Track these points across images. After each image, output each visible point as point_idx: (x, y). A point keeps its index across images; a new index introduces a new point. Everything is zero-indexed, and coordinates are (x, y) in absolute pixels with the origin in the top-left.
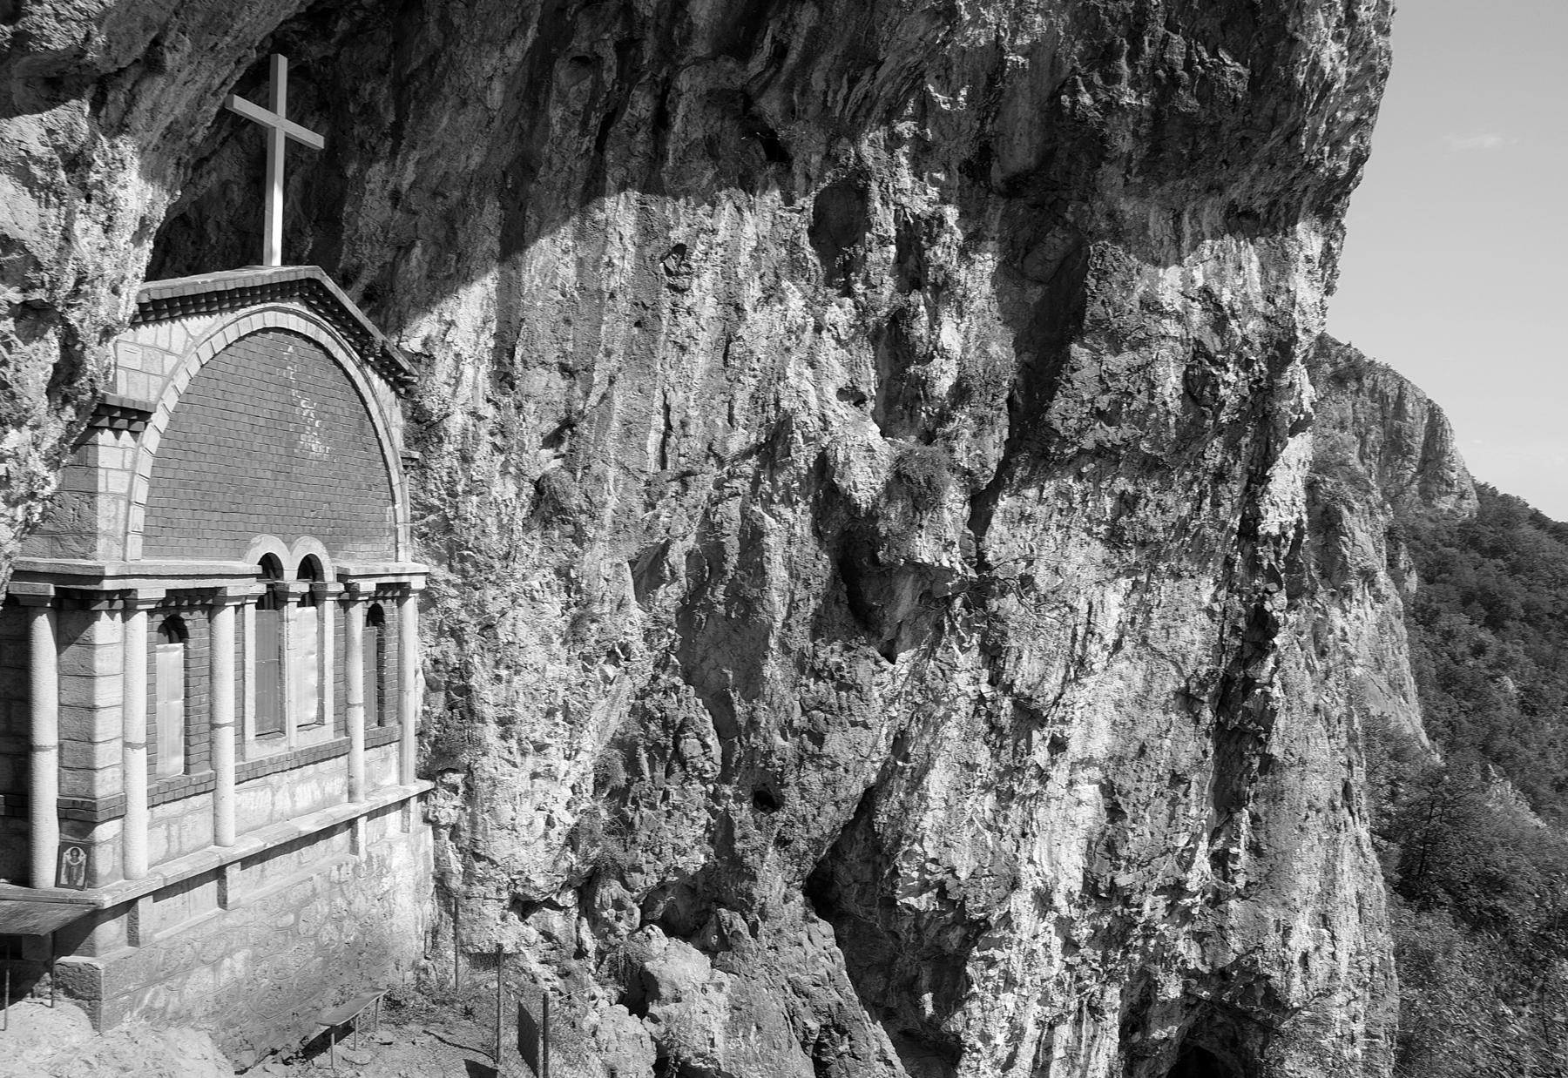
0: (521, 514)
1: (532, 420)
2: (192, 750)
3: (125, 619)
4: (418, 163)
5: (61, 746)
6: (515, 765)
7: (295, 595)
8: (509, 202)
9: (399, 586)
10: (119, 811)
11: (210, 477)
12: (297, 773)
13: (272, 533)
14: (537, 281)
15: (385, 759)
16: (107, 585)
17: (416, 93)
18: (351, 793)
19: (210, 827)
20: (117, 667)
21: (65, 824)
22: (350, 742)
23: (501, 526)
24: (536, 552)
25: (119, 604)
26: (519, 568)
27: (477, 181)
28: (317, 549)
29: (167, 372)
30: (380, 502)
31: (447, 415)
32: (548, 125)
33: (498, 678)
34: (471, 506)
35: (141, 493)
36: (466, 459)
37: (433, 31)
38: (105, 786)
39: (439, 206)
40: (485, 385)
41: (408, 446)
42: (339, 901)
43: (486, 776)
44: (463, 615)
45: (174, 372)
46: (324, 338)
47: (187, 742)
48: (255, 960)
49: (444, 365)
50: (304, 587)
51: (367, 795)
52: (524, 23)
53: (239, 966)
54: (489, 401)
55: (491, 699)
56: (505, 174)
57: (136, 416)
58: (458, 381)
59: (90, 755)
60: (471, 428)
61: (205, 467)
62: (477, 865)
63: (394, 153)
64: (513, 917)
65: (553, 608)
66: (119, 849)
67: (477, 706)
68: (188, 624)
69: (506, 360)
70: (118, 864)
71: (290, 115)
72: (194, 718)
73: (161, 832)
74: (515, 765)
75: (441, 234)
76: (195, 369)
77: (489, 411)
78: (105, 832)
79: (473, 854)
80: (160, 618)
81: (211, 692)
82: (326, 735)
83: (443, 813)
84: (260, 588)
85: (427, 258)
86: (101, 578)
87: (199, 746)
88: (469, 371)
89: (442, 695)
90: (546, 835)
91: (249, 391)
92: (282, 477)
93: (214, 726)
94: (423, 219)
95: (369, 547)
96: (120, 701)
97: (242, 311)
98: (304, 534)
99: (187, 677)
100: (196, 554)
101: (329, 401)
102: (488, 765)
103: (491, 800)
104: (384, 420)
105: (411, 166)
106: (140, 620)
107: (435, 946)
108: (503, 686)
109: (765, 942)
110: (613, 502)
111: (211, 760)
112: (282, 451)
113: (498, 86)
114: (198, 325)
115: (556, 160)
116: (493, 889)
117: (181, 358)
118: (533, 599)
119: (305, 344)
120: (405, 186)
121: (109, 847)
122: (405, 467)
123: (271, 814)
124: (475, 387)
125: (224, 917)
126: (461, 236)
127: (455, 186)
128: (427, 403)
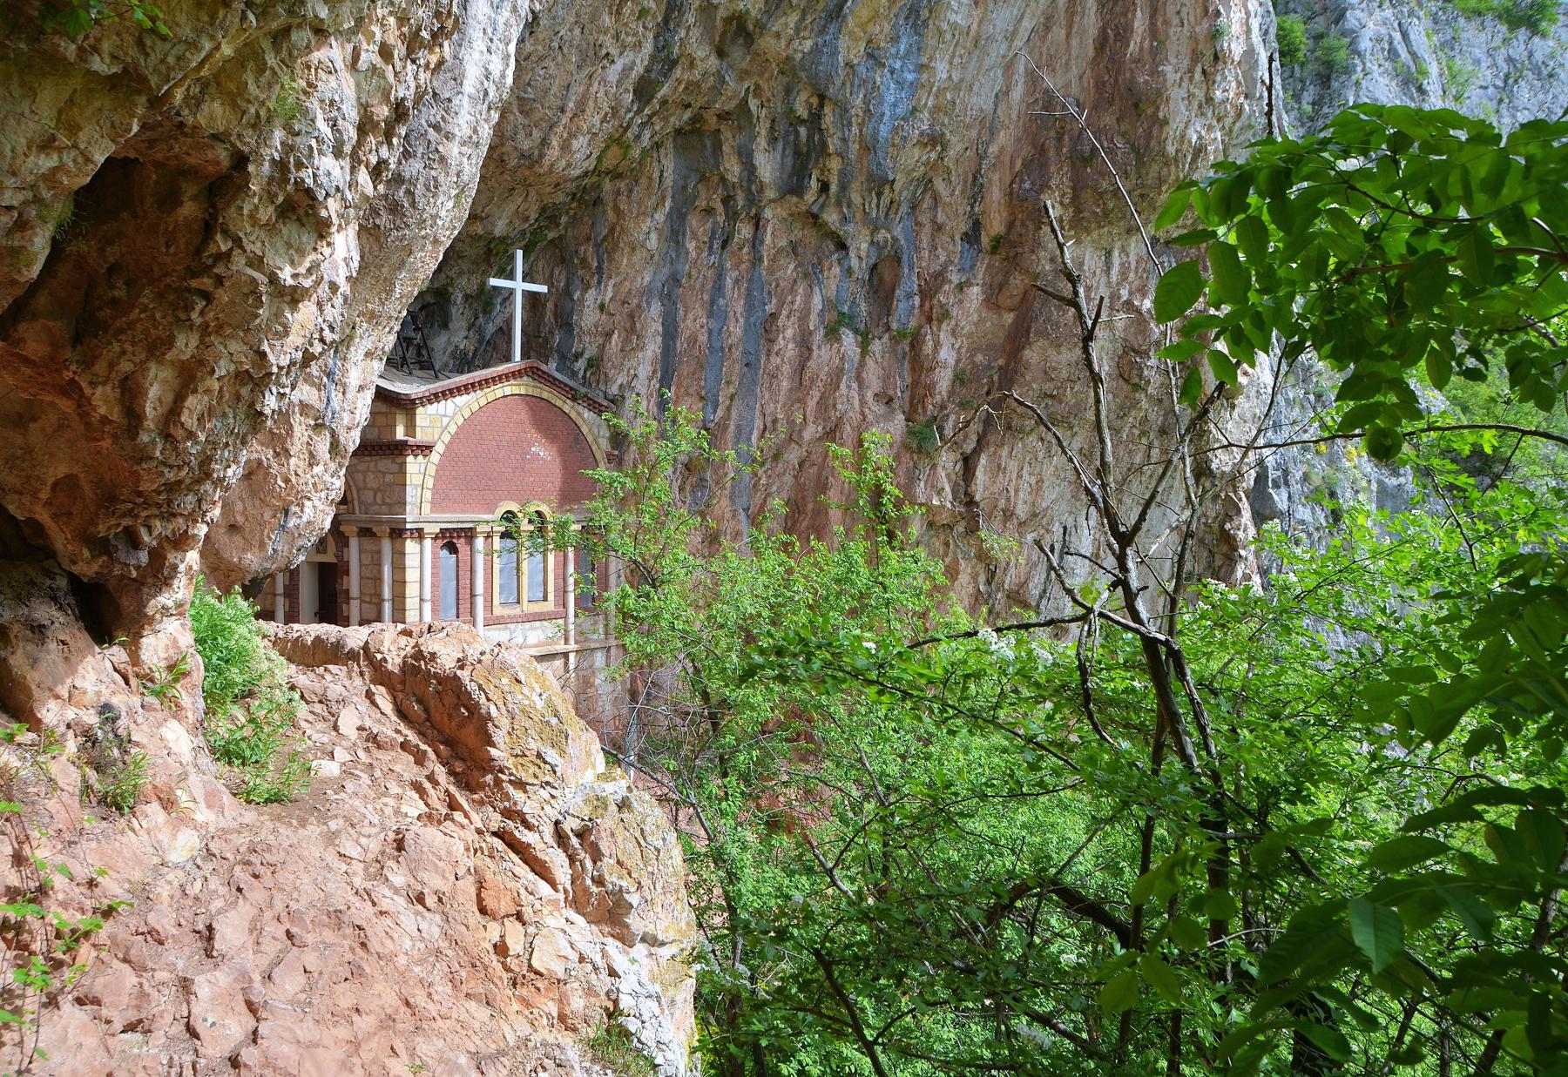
3: (421, 543)
12: (528, 625)
15: (595, 623)
16: (408, 526)
18: (566, 641)
27: (647, 292)
28: (544, 508)
35: (430, 483)
37: (611, 215)
39: (626, 309)
46: (545, 395)
52: (664, 198)
57: (426, 449)
59: (404, 604)
63: (599, 282)
71: (524, 280)
76: (460, 421)
80: (440, 543)
82: (549, 606)
87: (465, 606)
93: (473, 596)
94: (618, 317)
100: (463, 512)
105: (610, 288)
106: (428, 543)
111: (472, 613)
113: (654, 236)
114: (460, 400)
115: (694, 272)
117: (452, 418)
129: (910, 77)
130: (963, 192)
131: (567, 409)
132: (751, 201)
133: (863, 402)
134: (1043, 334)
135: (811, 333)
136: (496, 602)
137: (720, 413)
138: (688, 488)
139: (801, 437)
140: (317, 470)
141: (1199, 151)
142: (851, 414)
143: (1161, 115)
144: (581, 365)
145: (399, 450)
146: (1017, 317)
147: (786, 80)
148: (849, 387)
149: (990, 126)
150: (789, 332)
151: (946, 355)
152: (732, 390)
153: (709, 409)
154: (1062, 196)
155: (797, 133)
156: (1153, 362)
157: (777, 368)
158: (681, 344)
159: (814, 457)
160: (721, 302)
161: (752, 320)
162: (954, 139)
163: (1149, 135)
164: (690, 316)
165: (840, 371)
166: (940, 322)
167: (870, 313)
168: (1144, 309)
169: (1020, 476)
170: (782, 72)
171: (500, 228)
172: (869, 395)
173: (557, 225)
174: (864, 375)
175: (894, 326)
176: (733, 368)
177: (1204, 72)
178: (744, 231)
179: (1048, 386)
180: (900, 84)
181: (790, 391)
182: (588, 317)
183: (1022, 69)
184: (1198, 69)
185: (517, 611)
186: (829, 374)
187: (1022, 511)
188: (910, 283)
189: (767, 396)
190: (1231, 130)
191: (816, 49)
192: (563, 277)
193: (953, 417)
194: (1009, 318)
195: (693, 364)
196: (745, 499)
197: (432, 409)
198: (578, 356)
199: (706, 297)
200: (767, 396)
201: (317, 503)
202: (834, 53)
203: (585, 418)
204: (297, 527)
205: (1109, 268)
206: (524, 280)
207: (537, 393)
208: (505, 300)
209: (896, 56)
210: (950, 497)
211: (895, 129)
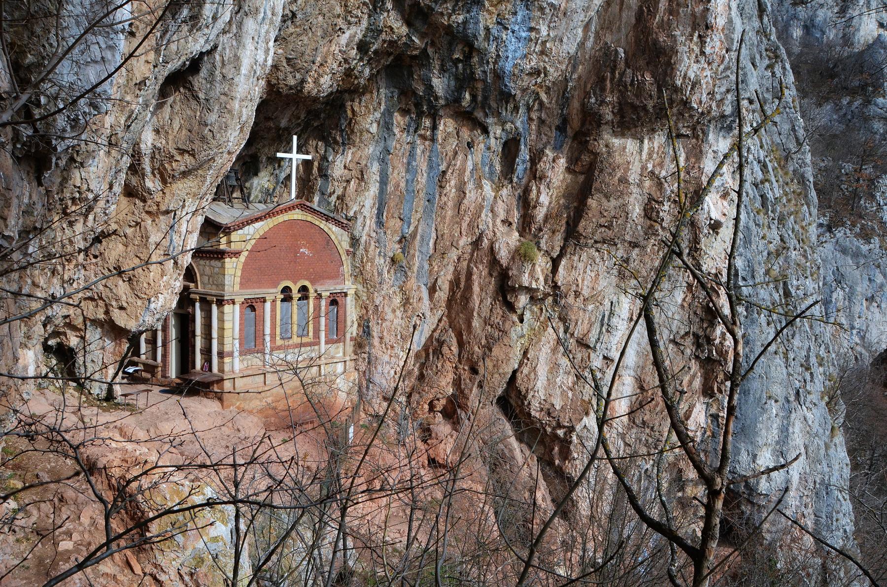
1: (389, 237)
4: (352, 153)
10: (231, 354)
15: (338, 347)
16: (226, 298)
20: (231, 318)
23: (378, 273)
26: (385, 287)
28: (307, 283)
34: (368, 267)
35: (239, 273)
36: (366, 251)
37: (349, 113)
38: (227, 348)
40: (374, 226)
46: (309, 219)
49: (360, 220)
57: (237, 254)
59: (223, 340)
62: (371, 385)
63: (344, 151)
65: (397, 300)
71: (297, 153)
77: (374, 235)
78: (227, 360)
79: (369, 381)
84: (282, 296)
87: (259, 341)
88: (368, 222)
93: (264, 335)
94: (354, 172)
100: (259, 288)
105: (350, 155)
106: (237, 307)
110: (417, 264)
114: (257, 225)
115: (398, 146)
128: (355, 233)
129: (524, 34)
130: (556, 102)
132: (431, 106)
133: (494, 225)
134: (599, 191)
135: (465, 183)
136: (278, 338)
138: (392, 271)
139: (458, 244)
141: (695, 84)
142: (487, 232)
143: (672, 61)
144: (333, 199)
145: (220, 255)
146: (586, 178)
147: (449, 38)
148: (487, 216)
149: (573, 61)
150: (453, 183)
151: (544, 199)
152: (419, 215)
154: (613, 108)
155: (457, 68)
156: (666, 208)
157: (445, 203)
158: (390, 188)
159: (466, 255)
160: (414, 163)
161: (431, 175)
162: (552, 70)
163: (665, 74)
164: (396, 172)
165: (481, 207)
166: (540, 179)
167: (502, 171)
168: (662, 176)
169: (585, 272)
170: (447, 34)
171: (284, 123)
172: (498, 222)
173: (319, 118)
174: (496, 209)
175: (515, 180)
176: (420, 203)
177: (700, 36)
178: (427, 122)
179: (602, 221)
180: (518, 39)
181: (452, 217)
182: (337, 170)
183: (593, 28)
184: (696, 34)
186: (475, 208)
187: (586, 292)
188: (524, 154)
189: (439, 219)
190: (717, 70)
191: (465, 22)
193: (546, 236)
194: (581, 178)
196: (425, 279)
198: (330, 196)
199: (405, 161)
200: (439, 219)
202: (477, 23)
203: (334, 231)
205: (641, 151)
206: (297, 153)
207: (304, 218)
209: (516, 23)
210: (543, 283)
211: (515, 65)
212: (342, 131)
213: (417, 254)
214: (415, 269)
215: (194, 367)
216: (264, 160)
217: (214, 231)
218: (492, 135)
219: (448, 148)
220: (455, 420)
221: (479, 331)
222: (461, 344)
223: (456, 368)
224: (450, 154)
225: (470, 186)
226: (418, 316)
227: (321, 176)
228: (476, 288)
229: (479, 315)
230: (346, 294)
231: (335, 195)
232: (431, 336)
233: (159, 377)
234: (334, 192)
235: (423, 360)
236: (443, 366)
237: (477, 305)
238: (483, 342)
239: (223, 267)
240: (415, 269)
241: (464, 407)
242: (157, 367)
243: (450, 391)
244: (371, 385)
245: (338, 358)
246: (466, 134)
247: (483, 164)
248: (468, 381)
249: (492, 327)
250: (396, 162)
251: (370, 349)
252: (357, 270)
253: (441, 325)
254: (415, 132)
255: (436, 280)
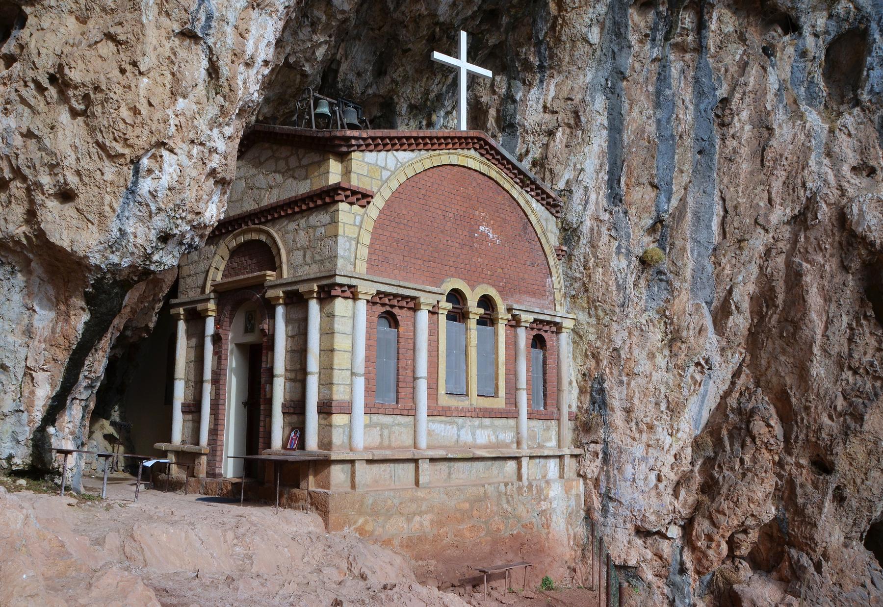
0: (631, 279)
1: (634, 219)
2: (400, 390)
4: (556, 86)
5: (320, 373)
6: (634, 439)
7: (474, 313)
8: (610, 95)
9: (556, 324)
10: (347, 409)
11: (415, 240)
12: (477, 422)
13: (462, 279)
14: (633, 137)
15: (548, 429)
16: (339, 280)
17: (548, 44)
18: (518, 443)
19: (412, 437)
20: (349, 330)
21: (321, 416)
22: (518, 412)
23: (618, 286)
24: (643, 302)
25: (348, 294)
26: (632, 311)
28: (492, 292)
29: (384, 178)
30: (542, 275)
31: (582, 222)
32: (630, 47)
33: (621, 383)
35: (366, 239)
38: (339, 394)
40: (604, 203)
41: (561, 244)
42: (505, 506)
43: (615, 446)
44: (599, 344)
45: (388, 178)
46: (493, 174)
47: (398, 386)
48: (440, 523)
50: (481, 311)
51: (529, 448)
53: (426, 523)
54: (606, 210)
55: (617, 395)
56: (607, 80)
57: (363, 197)
58: (587, 202)
59: (331, 376)
60: (596, 228)
61: (412, 234)
62: (611, 504)
63: (541, 81)
64: (639, 542)
65: (656, 336)
66: (347, 433)
67: (608, 399)
68: (398, 318)
69: (616, 186)
70: (346, 441)
72: (402, 372)
73: (376, 431)
74: (634, 439)
75: (572, 122)
76: (403, 179)
77: (606, 216)
78: (338, 420)
79: (607, 497)
80: (380, 309)
81: (414, 360)
82: (500, 402)
83: (589, 471)
85: (566, 136)
86: (335, 275)
87: (405, 391)
88: (593, 196)
89: (588, 396)
90: (656, 486)
91: (443, 197)
92: (467, 248)
93: (415, 379)
94: (561, 116)
95: (533, 300)
96: (350, 349)
97: (432, 153)
98: (483, 283)
99: (398, 348)
101: (500, 211)
102: (615, 438)
103: (619, 462)
104: (542, 227)
105: (552, 88)
106: (362, 306)
107: (584, 556)
108: (624, 387)
109: (830, 580)
111: (414, 398)
112: (466, 233)
113: (596, 30)
114: (404, 156)
115: (637, 65)
116: (621, 521)
117: (393, 173)
118: (642, 330)
119: (481, 175)
120: (550, 99)
121: (341, 430)
122: (558, 255)
123: (457, 440)
124: (597, 203)
125: (416, 491)
126: (583, 119)
127: (578, 92)
128: (569, 217)
131: (515, 194)
133: (838, 175)
135: (768, 113)
136: (442, 390)
137: (674, 202)
138: (642, 283)
139: (768, 221)
140: (181, 103)
148: (820, 164)
150: (745, 115)
152: (685, 178)
153: (663, 198)
157: (735, 151)
158: (628, 136)
159: (780, 245)
160: (668, 92)
164: (636, 110)
174: (837, 149)
178: (687, 19)
181: (752, 173)
185: (463, 403)
192: (505, 85)
195: (644, 153)
196: (708, 291)
197: (371, 157)
199: (651, 89)
201: (183, 159)
203: (536, 210)
204: (153, 195)
207: (484, 169)
208: (448, 113)
212: (539, 43)
213: (689, 245)
214: (688, 273)
215: (268, 444)
216: (404, 109)
217: (317, 158)
218: (807, 30)
219: (728, 60)
220: (786, 572)
221: (827, 384)
222: (787, 416)
223: (780, 464)
224: (733, 69)
225: (779, 118)
226: (698, 364)
227: (502, 130)
228: (814, 299)
229: (824, 351)
230: (558, 328)
231: (530, 158)
232: (721, 407)
233: (202, 475)
234: (527, 152)
235: (710, 453)
236: (754, 460)
237: (819, 332)
238: (840, 403)
239: (334, 222)
240: (688, 273)
241: (808, 545)
242: (199, 454)
243: (769, 512)
244: (611, 504)
245: (550, 448)
246: (755, 37)
247: (795, 83)
248: (810, 488)
249: (855, 372)
250: (636, 93)
251: (607, 434)
252: (577, 285)
253: (741, 382)
254: (666, 38)
255: (730, 292)
